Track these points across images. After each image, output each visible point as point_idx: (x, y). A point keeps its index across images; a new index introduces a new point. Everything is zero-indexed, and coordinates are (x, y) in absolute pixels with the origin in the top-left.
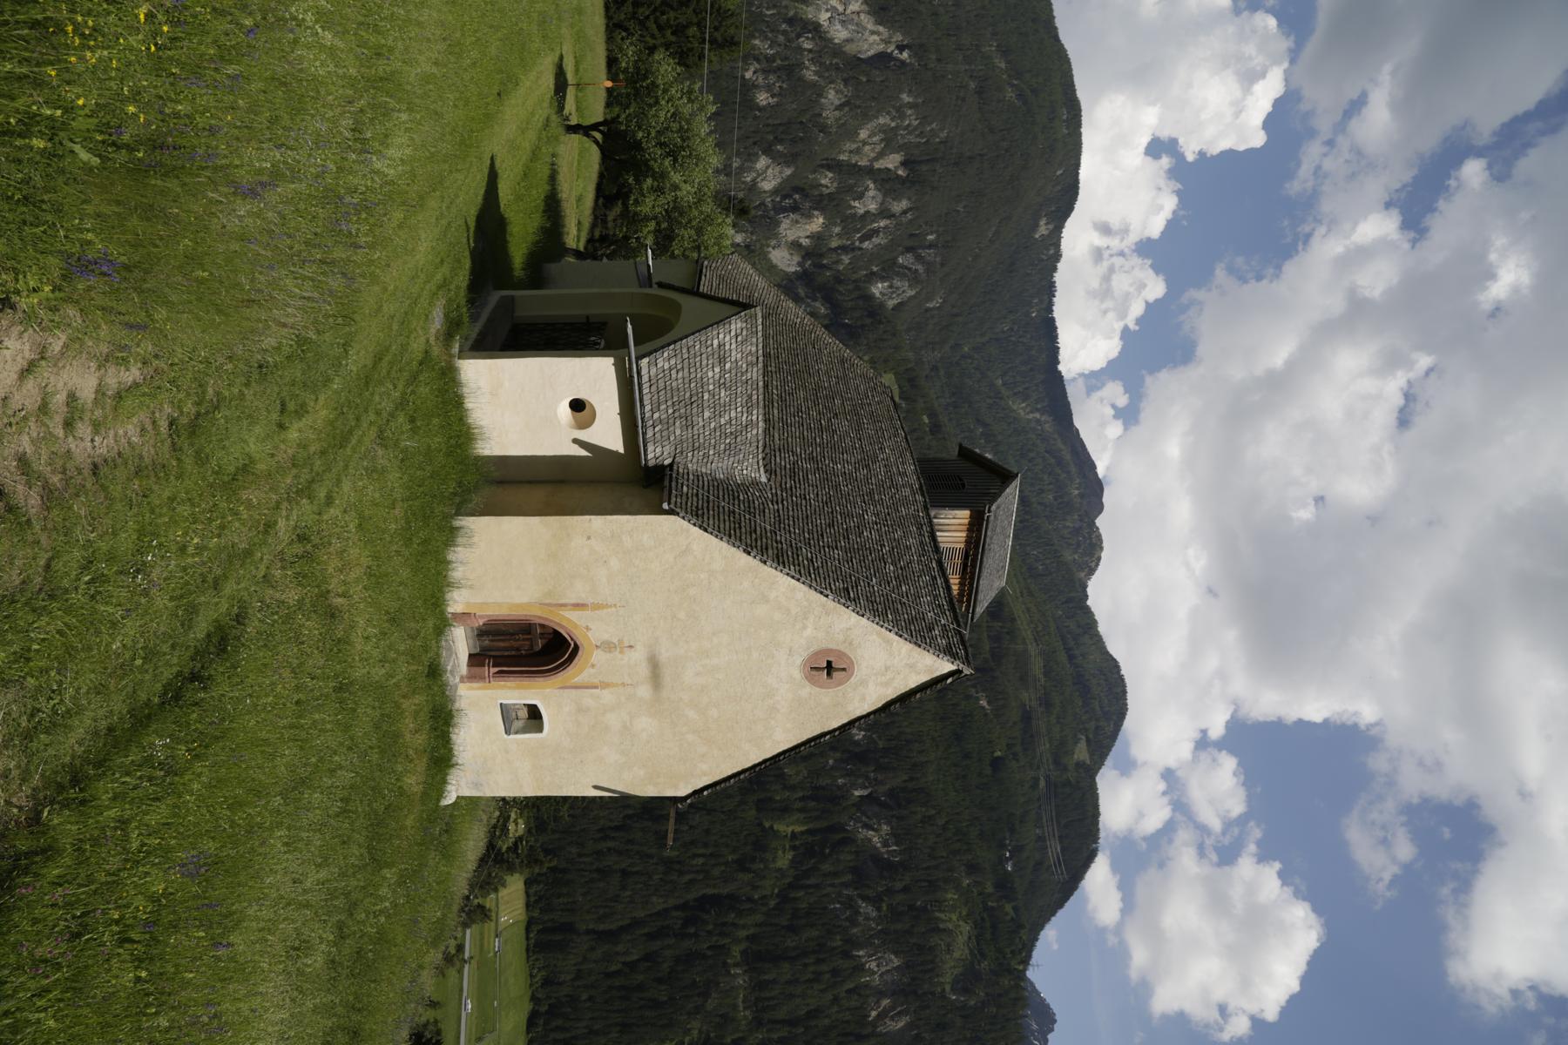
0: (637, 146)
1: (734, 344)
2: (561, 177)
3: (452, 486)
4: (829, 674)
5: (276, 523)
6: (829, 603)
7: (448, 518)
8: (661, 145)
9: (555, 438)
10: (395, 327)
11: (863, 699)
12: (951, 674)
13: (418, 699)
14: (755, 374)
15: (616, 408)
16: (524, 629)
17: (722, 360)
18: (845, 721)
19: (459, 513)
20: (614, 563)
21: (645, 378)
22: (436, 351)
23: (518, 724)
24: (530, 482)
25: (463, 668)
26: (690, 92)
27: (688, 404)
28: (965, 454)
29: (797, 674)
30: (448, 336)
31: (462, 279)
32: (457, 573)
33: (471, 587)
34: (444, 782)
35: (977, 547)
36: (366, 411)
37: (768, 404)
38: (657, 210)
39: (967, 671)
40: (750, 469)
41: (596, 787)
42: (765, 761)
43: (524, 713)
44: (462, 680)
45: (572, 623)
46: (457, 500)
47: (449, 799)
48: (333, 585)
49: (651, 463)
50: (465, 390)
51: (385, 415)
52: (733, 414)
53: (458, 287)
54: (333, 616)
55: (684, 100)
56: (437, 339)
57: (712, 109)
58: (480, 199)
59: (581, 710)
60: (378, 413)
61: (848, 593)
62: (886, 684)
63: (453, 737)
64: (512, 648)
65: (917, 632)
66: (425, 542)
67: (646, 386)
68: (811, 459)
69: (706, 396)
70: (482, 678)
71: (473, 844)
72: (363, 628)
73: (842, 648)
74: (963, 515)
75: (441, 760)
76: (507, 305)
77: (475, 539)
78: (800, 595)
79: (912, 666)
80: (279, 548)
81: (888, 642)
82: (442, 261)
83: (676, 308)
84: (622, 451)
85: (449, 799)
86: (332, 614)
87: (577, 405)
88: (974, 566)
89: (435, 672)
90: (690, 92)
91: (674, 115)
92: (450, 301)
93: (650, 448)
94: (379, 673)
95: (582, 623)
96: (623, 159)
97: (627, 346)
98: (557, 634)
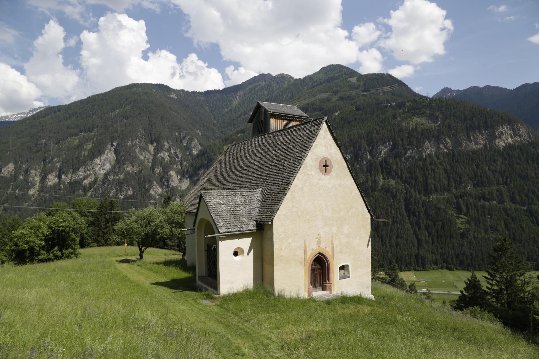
0: (147, 235)
1: (214, 200)
2: (158, 261)
3: (264, 297)
4: (327, 166)
5: (277, 357)
6: (303, 166)
7: (275, 298)
8: (146, 226)
9: (247, 261)
10: (209, 317)
11: (336, 154)
12: (327, 124)
13: (338, 308)
14: (224, 193)
15: (237, 240)
16: (313, 271)
17: (220, 204)
18: (344, 160)
19: (273, 295)
20: (290, 240)
21: (226, 230)
22: (217, 302)
23: (346, 273)
24: (262, 270)
26: (128, 217)
27: (235, 215)
28: (251, 121)
29: (328, 177)
30: (212, 298)
31: (193, 294)
32: (294, 295)
33: (299, 290)
34: (366, 299)
35: (283, 116)
36: (238, 326)
37: (234, 188)
38: (168, 227)
39: (326, 118)
40: (257, 194)
41: (368, 246)
42: (358, 188)
43: (342, 271)
44: (331, 293)
45: (311, 255)
46: (269, 295)
47: (373, 297)
48: (298, 337)
49: (255, 228)
50: (231, 292)
51: (239, 320)
52: (238, 200)
53: (196, 295)
54: (309, 337)
55: (131, 219)
56: (213, 302)
57: (134, 209)
58: (165, 288)
59: (341, 252)
60: (239, 322)
61: (299, 160)
62: (331, 147)
63: (351, 296)
64: (320, 276)
65: (312, 136)
66: (283, 306)
67: (229, 230)
68: (253, 173)
69: (232, 209)
70: (330, 286)
71: (388, 289)
72: (313, 327)
73: (318, 162)
74: (272, 121)
75: (359, 300)
76: (202, 278)
77: (282, 288)
78: (300, 176)
79: (325, 137)
80: (286, 356)
81: (316, 146)
82: (187, 301)
83: (202, 220)
84: (251, 238)
85: (373, 297)
86: (309, 337)
87: (236, 254)
88: (290, 117)
89: (328, 302)
90: (128, 217)
91: (136, 222)
92: (200, 298)
93: (250, 228)
94: (329, 321)
96: (151, 240)
97: (215, 237)
98: (315, 260)
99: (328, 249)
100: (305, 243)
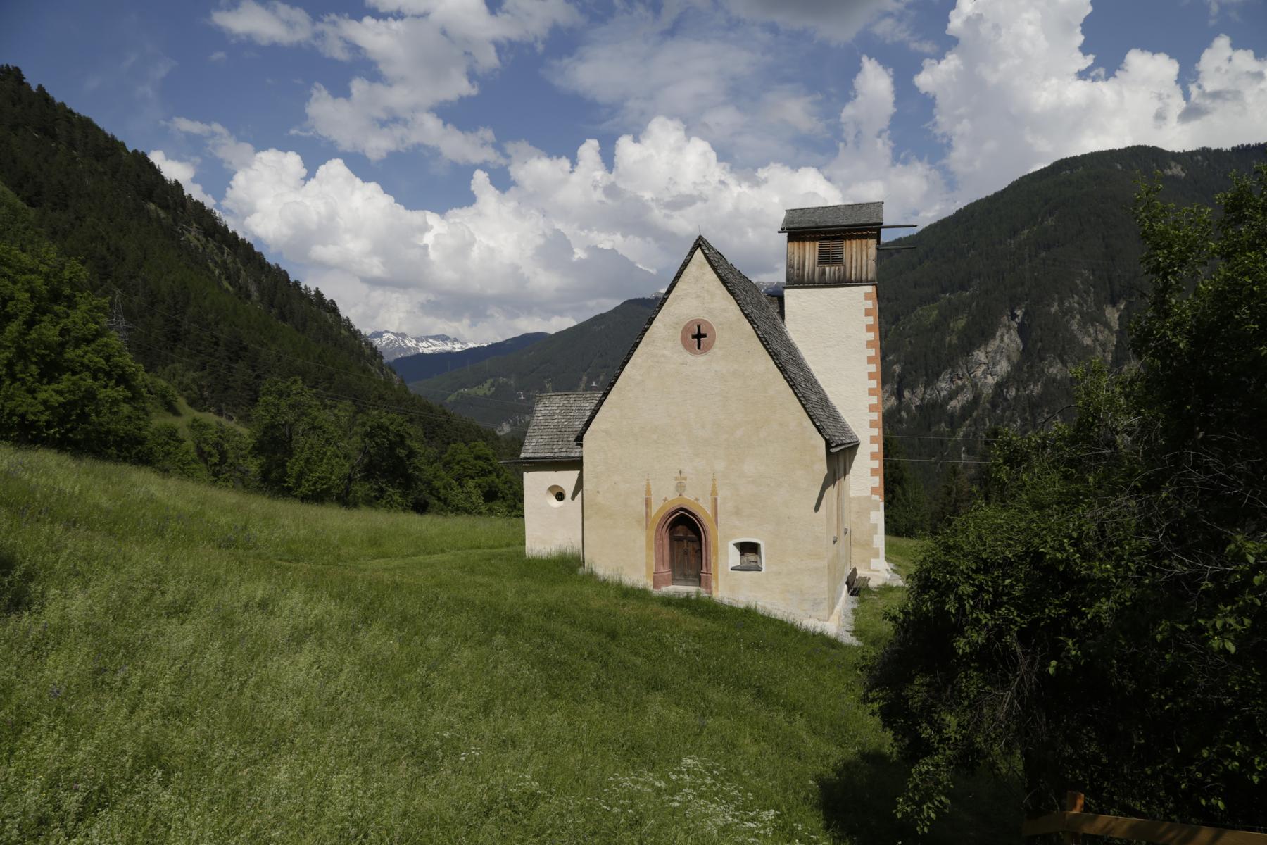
17: (553, 414)
25: (702, 590)
29: (703, 358)
35: (818, 232)
41: (817, 509)
63: (742, 606)
78: (639, 360)
88: (835, 232)
95: (661, 504)
99: (701, 502)
100: (648, 485)
